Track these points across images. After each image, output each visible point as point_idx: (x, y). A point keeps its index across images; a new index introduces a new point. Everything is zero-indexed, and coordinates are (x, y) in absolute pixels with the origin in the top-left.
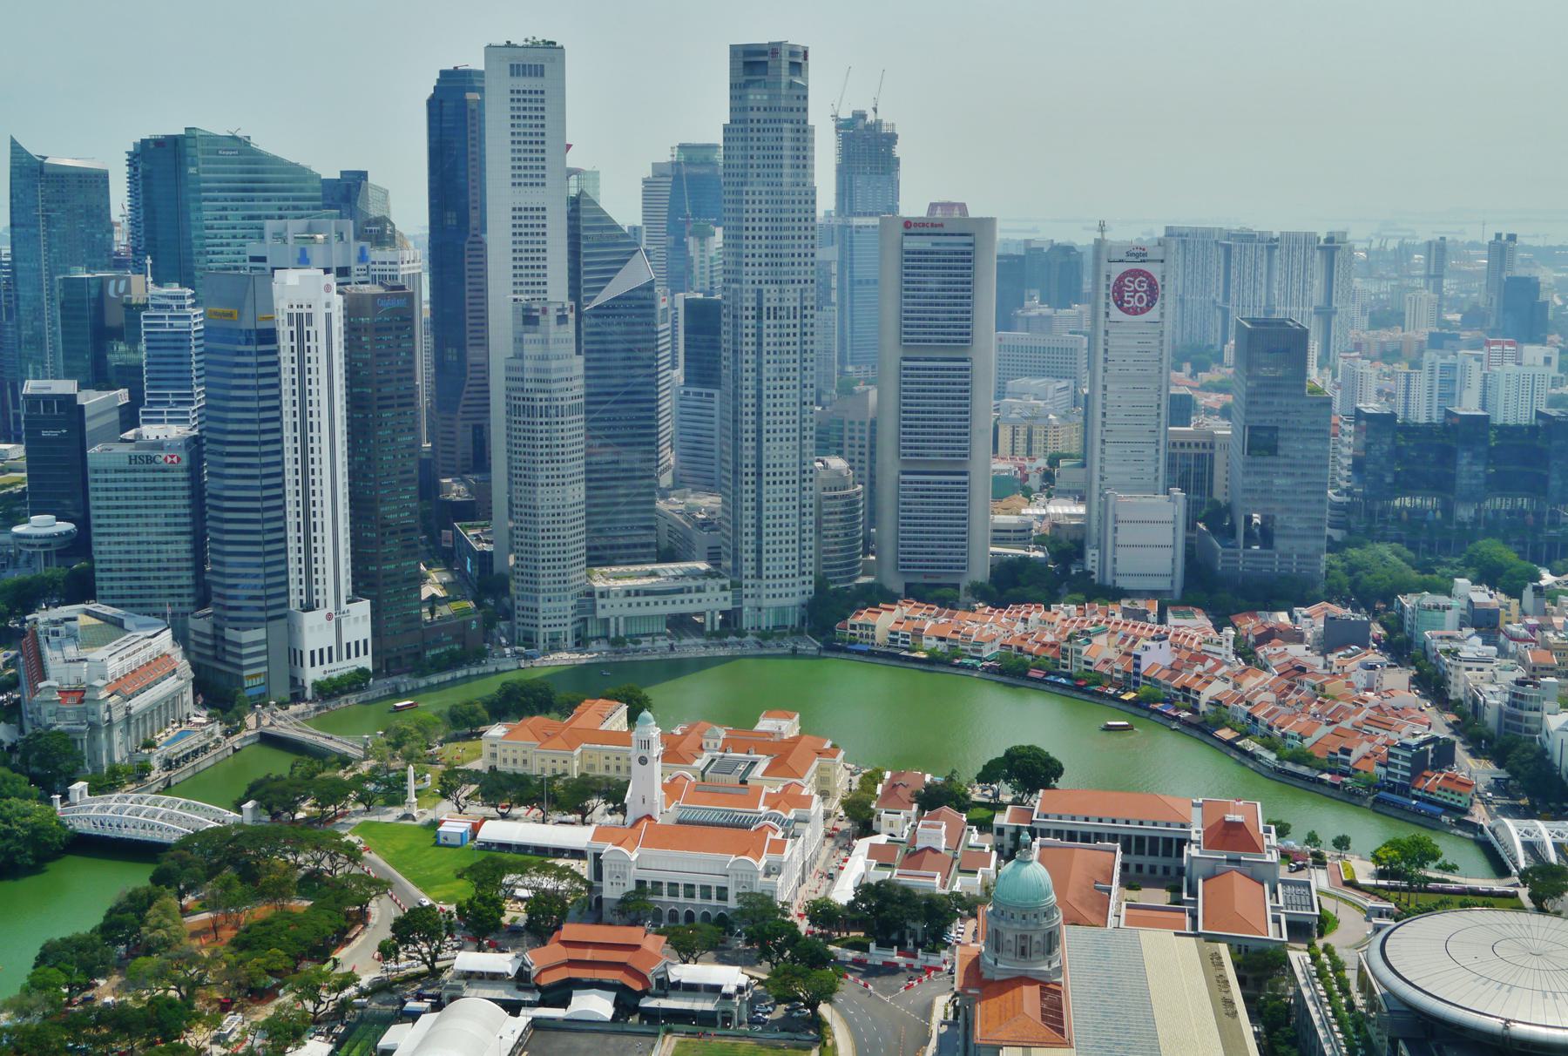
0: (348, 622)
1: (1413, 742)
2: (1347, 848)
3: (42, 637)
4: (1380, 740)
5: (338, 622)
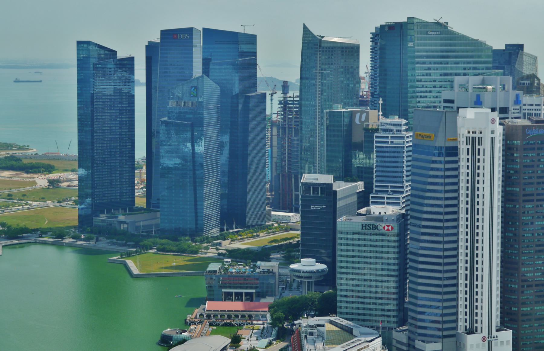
0: (496, 344)
3: (303, 335)
5: (490, 344)
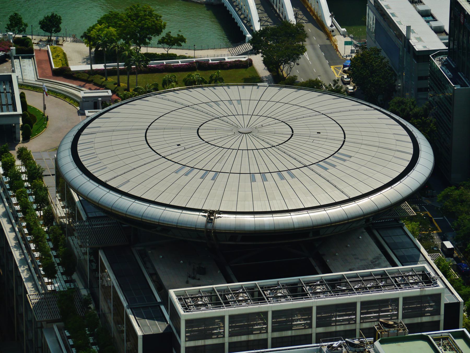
2: (58, 30)
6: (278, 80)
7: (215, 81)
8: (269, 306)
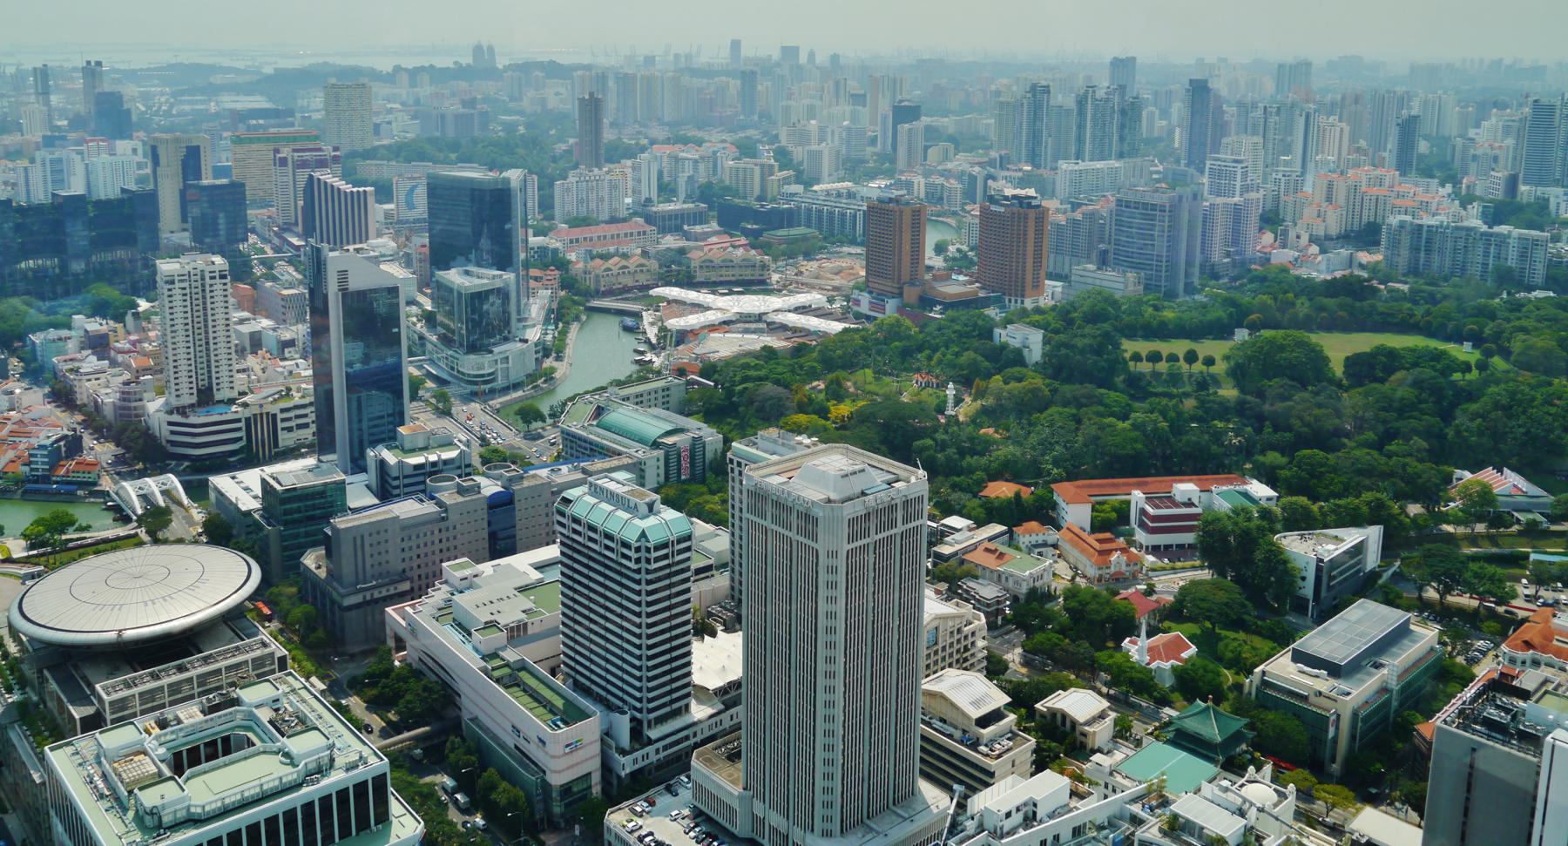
1: (48, 442)
4: (22, 447)
6: (156, 541)
7: (114, 549)
8: (165, 681)
